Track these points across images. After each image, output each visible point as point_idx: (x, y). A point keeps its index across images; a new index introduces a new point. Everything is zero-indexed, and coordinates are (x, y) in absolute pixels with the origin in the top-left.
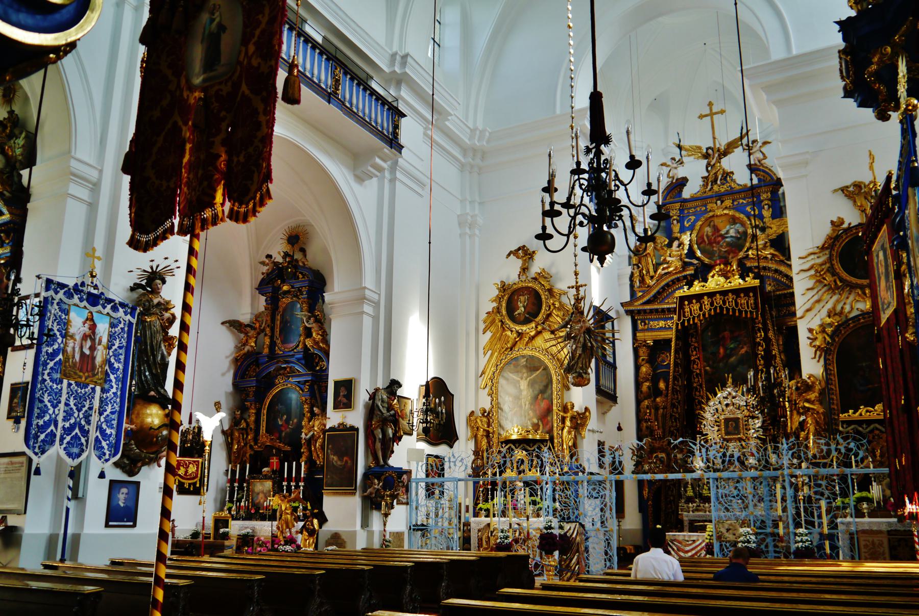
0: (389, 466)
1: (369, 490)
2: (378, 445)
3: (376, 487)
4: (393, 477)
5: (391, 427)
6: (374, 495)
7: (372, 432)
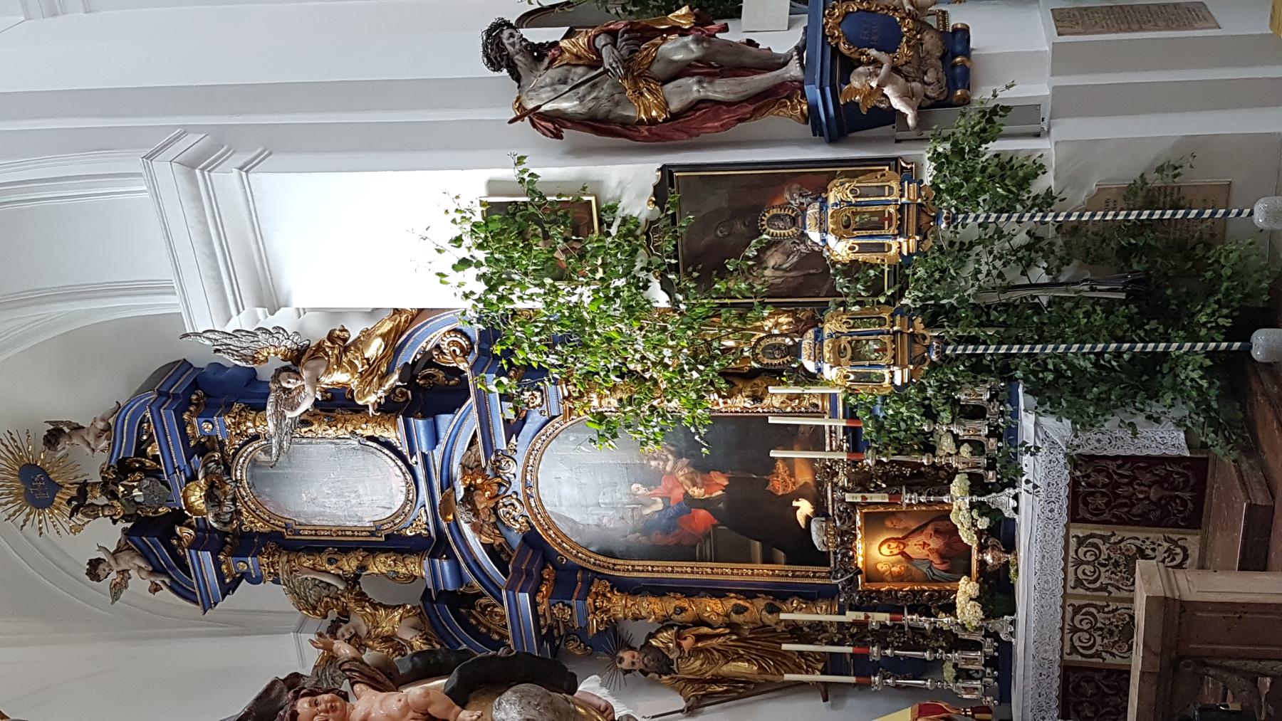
0: (800, 49)
1: (897, 104)
2: (721, 90)
3: (883, 71)
4: (847, 14)
5: (657, 46)
6: (916, 85)
7: (675, 116)
